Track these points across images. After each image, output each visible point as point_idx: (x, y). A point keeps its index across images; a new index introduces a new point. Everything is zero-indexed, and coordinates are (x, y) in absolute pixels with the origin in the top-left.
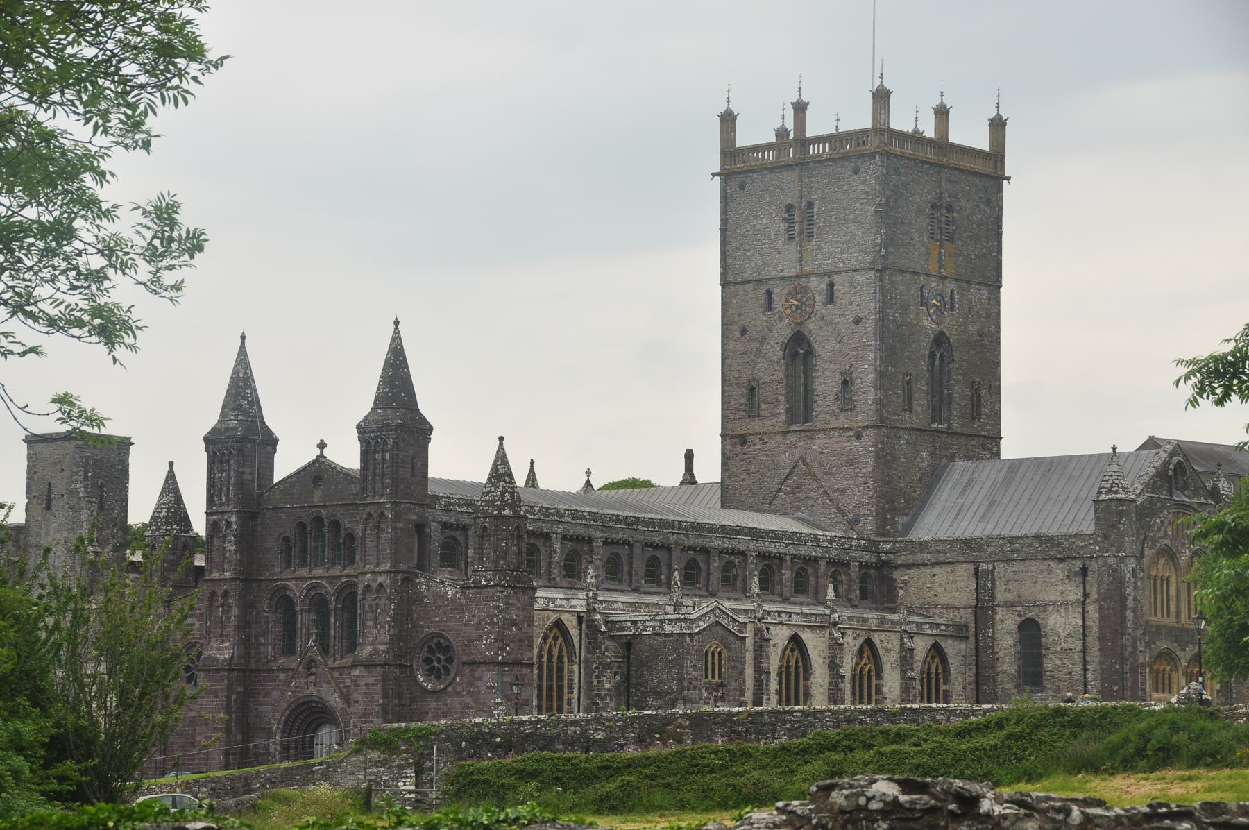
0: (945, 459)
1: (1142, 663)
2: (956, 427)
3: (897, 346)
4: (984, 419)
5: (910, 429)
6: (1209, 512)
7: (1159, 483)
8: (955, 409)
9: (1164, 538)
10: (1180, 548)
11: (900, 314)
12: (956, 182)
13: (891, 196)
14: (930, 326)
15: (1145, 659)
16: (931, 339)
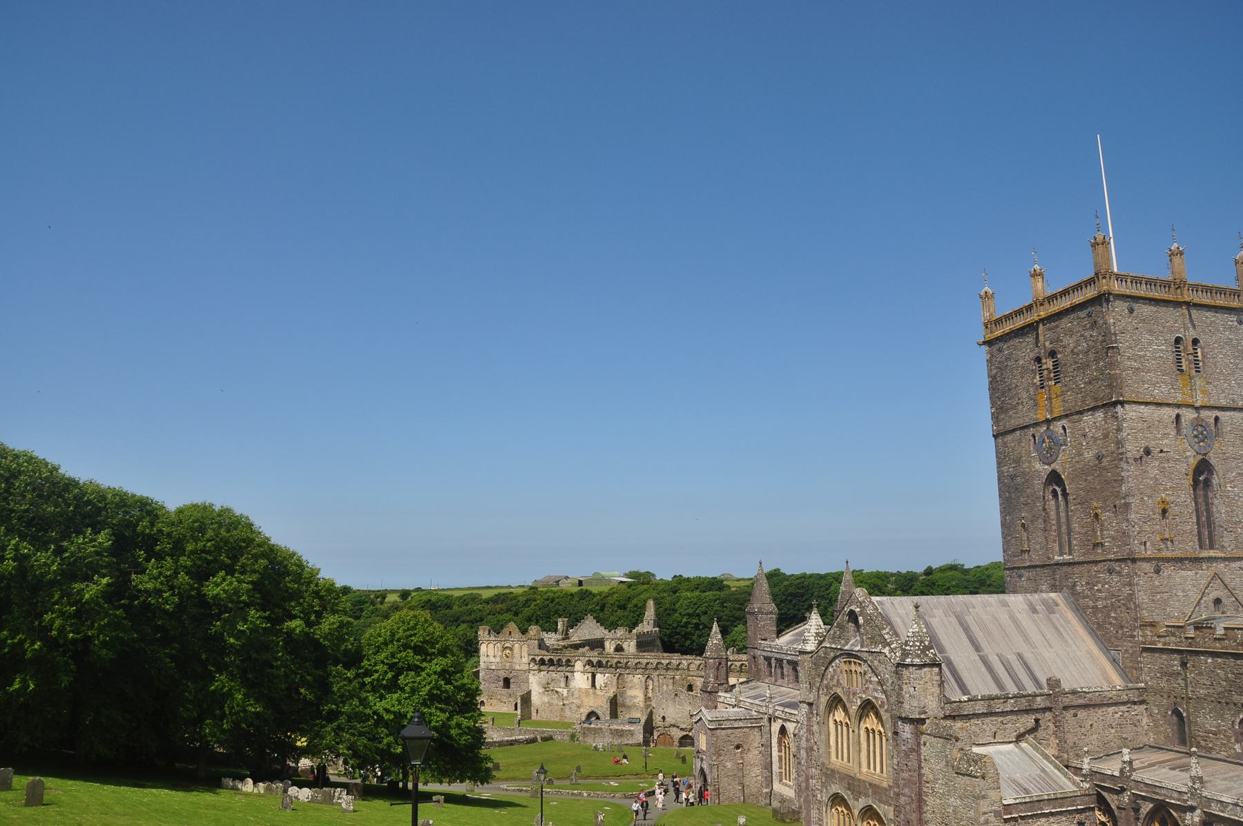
0: (1065, 588)
1: (820, 801)
2: (1076, 557)
3: (1013, 496)
4: (1109, 542)
5: (1029, 567)
6: (879, 661)
7: (838, 633)
8: (1075, 539)
9: (837, 686)
10: (851, 697)
11: (1013, 467)
12: (1057, 327)
13: (997, 373)
14: (1044, 469)
15: (822, 798)
16: (1044, 480)
